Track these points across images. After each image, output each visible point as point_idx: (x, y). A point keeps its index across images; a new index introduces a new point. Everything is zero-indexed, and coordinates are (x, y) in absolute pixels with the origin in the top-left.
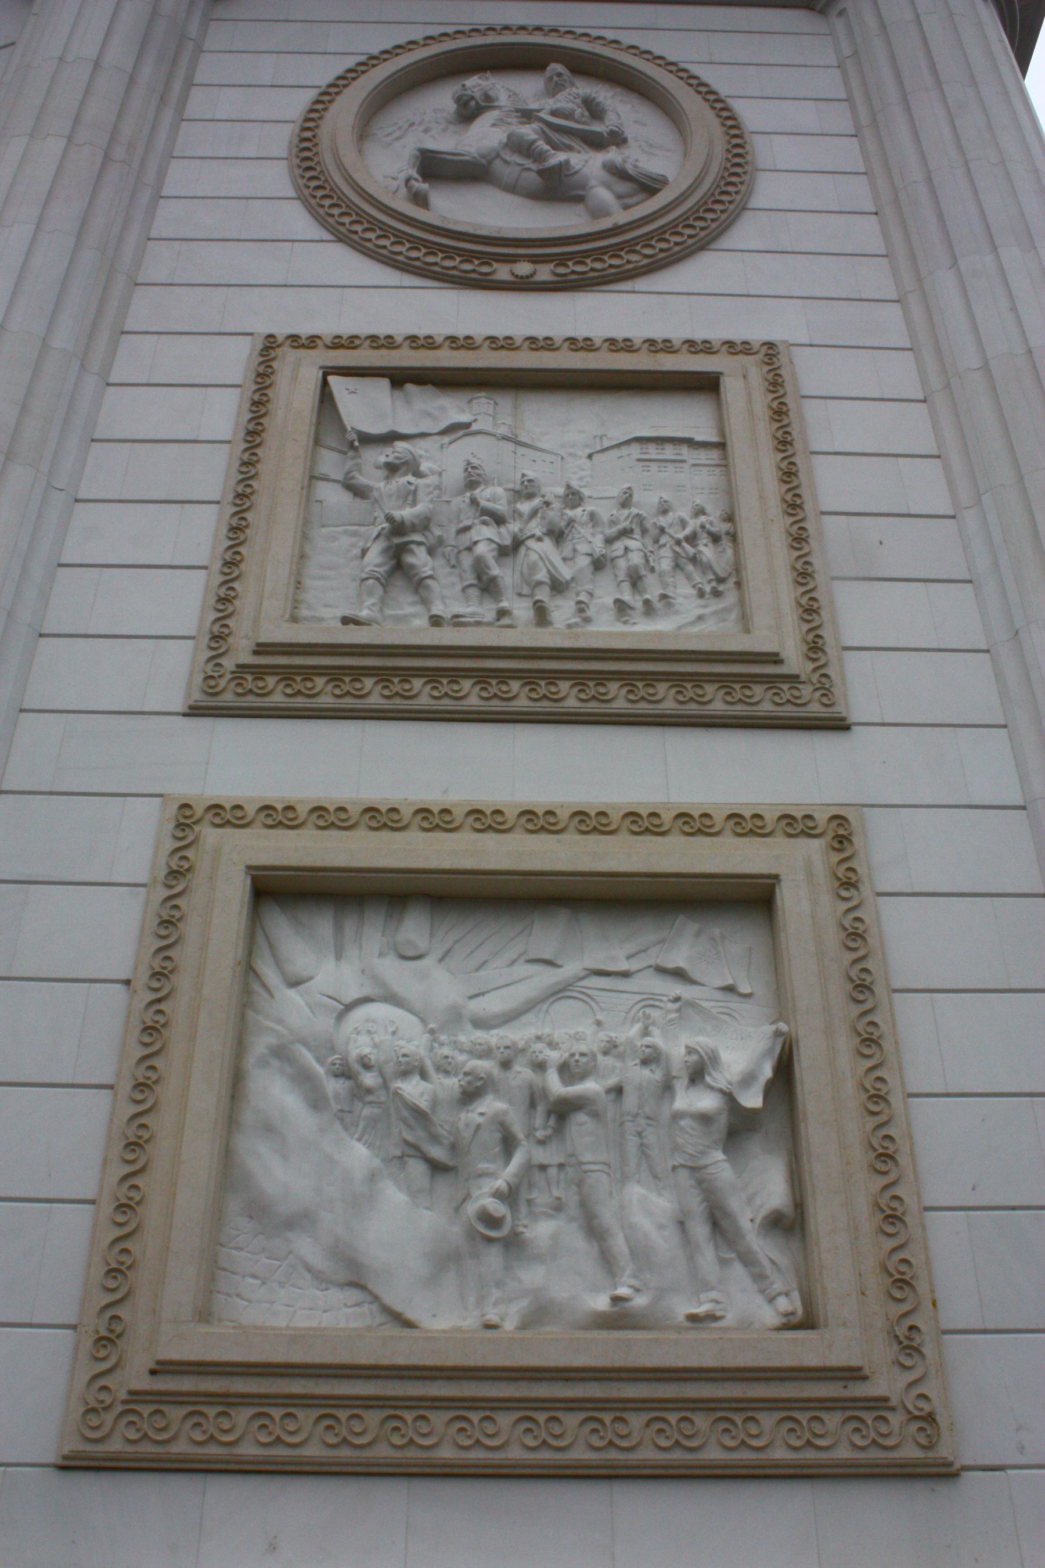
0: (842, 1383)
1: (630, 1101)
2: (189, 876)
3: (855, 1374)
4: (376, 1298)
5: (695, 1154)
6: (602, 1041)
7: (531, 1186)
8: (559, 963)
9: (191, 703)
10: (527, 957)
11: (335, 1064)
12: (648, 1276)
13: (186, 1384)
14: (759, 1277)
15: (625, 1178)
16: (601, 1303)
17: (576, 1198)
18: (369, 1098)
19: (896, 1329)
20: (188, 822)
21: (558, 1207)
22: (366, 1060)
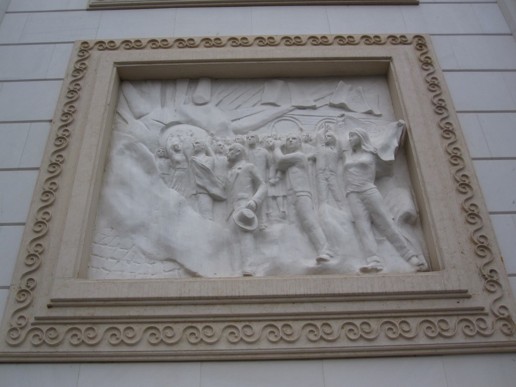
0: (457, 300)
1: (321, 163)
2: (84, 71)
3: (464, 295)
4: (182, 266)
5: (359, 185)
6: (304, 136)
7: (268, 207)
8: (278, 104)
9: (91, 4)
10: (262, 103)
11: (159, 151)
12: (337, 248)
13: (69, 312)
14: (400, 248)
15: (320, 201)
16: (312, 263)
17: (294, 211)
18: (178, 166)
19: (483, 271)
20: (86, 49)
21: (284, 217)
22: (176, 147)
